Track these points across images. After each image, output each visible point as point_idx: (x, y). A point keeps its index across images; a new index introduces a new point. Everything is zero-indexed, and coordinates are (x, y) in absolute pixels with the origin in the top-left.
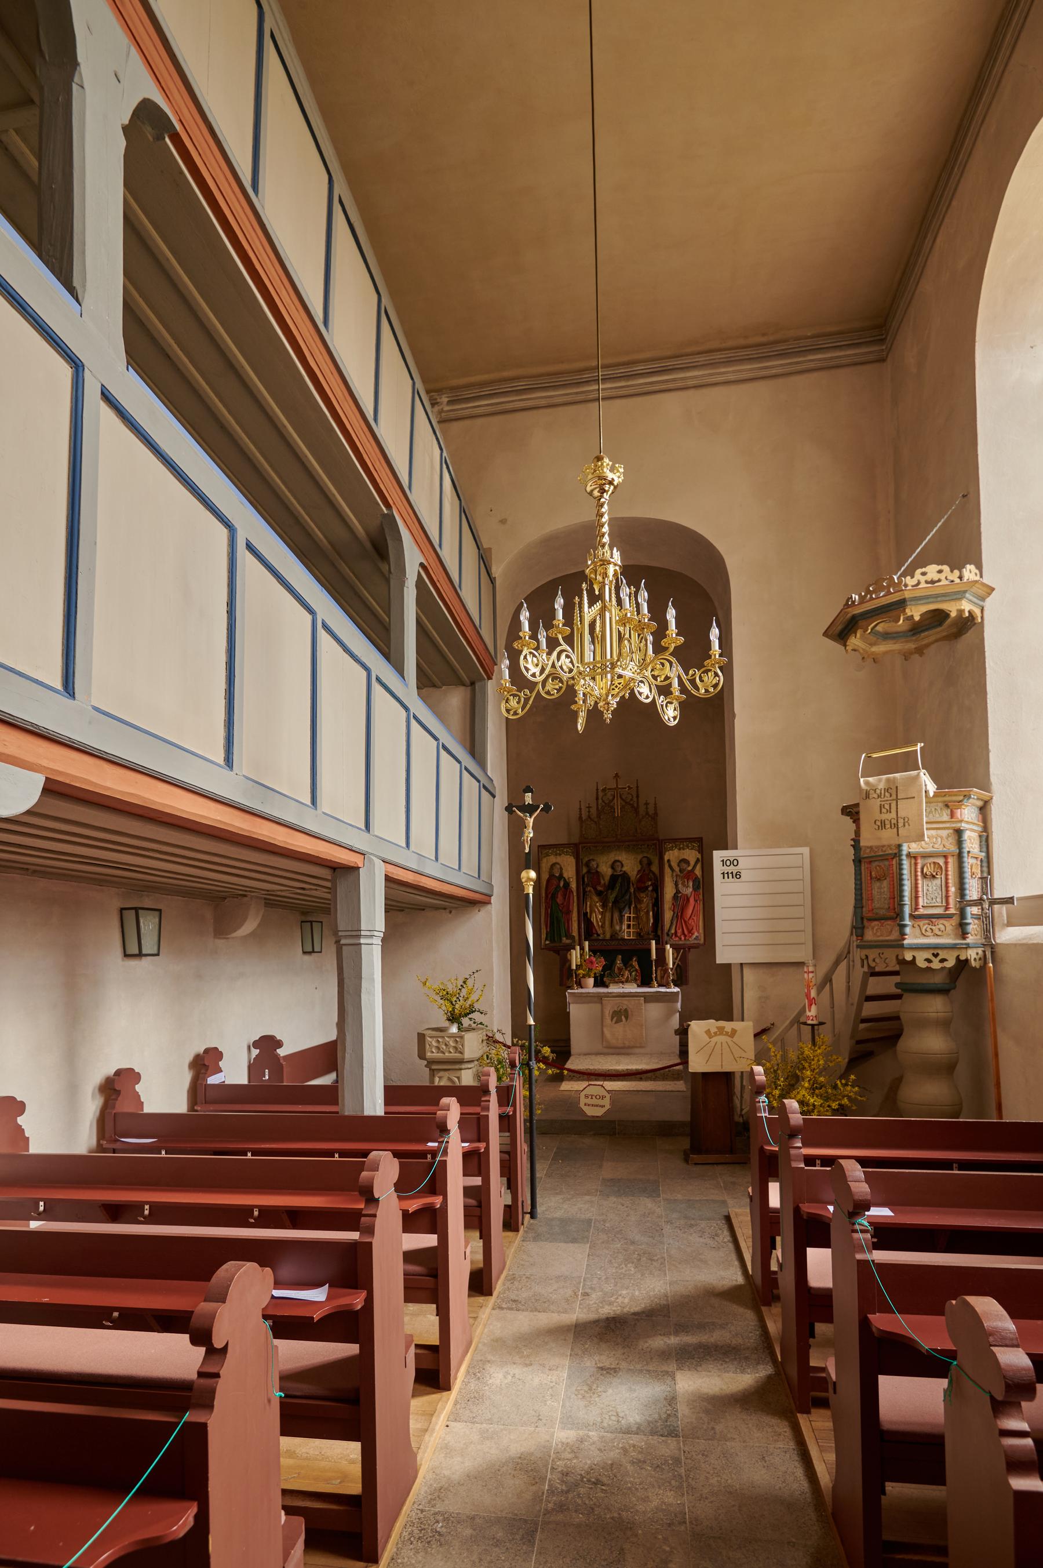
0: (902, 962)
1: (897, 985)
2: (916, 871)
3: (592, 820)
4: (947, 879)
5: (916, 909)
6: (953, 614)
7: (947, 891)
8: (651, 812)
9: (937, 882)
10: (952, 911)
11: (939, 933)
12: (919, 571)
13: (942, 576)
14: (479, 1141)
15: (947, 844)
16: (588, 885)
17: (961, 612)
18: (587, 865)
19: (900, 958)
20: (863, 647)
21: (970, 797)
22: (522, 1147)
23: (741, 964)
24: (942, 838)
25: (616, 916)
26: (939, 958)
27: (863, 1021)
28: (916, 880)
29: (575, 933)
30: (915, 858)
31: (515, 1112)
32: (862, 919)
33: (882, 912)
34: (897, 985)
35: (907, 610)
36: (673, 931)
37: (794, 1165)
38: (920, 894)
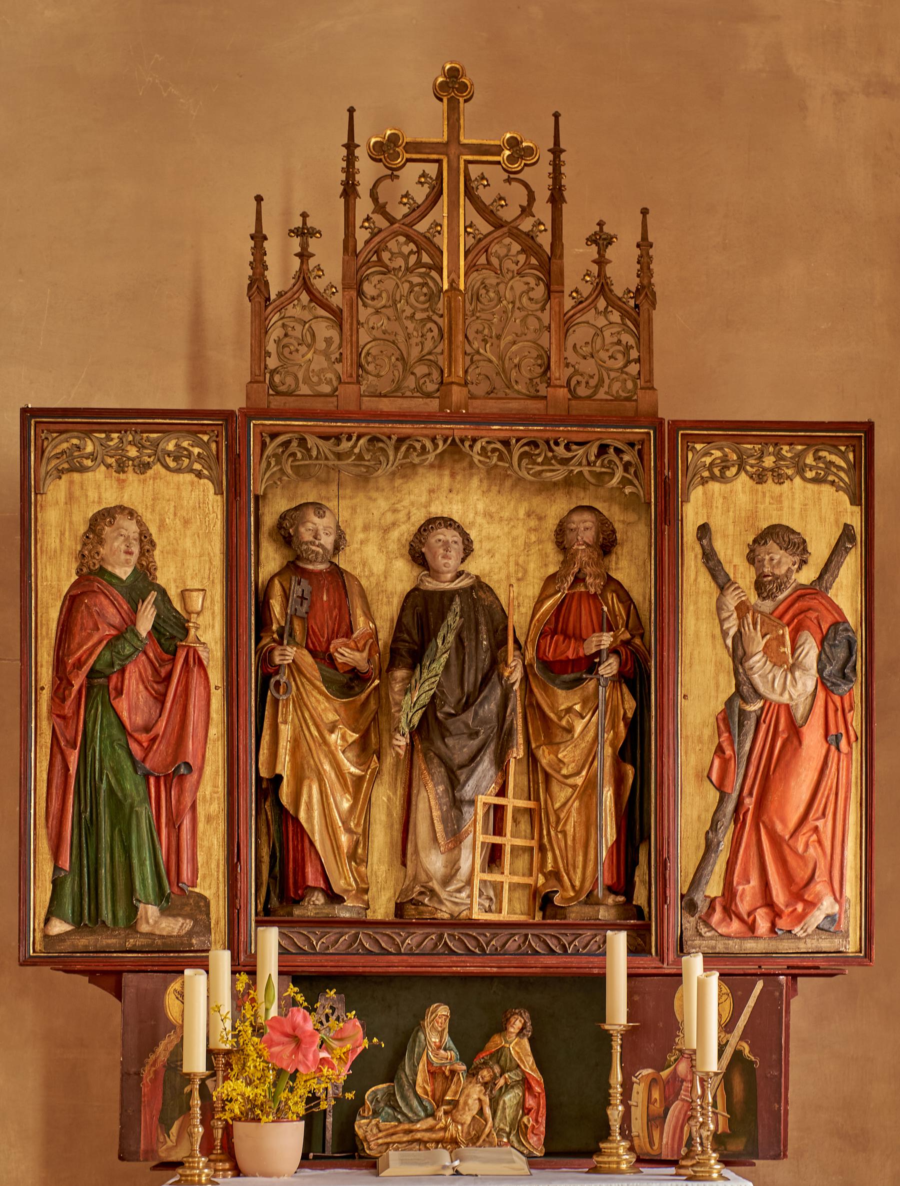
8: (623, 275)
16: (284, 636)
18: (286, 535)
25: (430, 799)
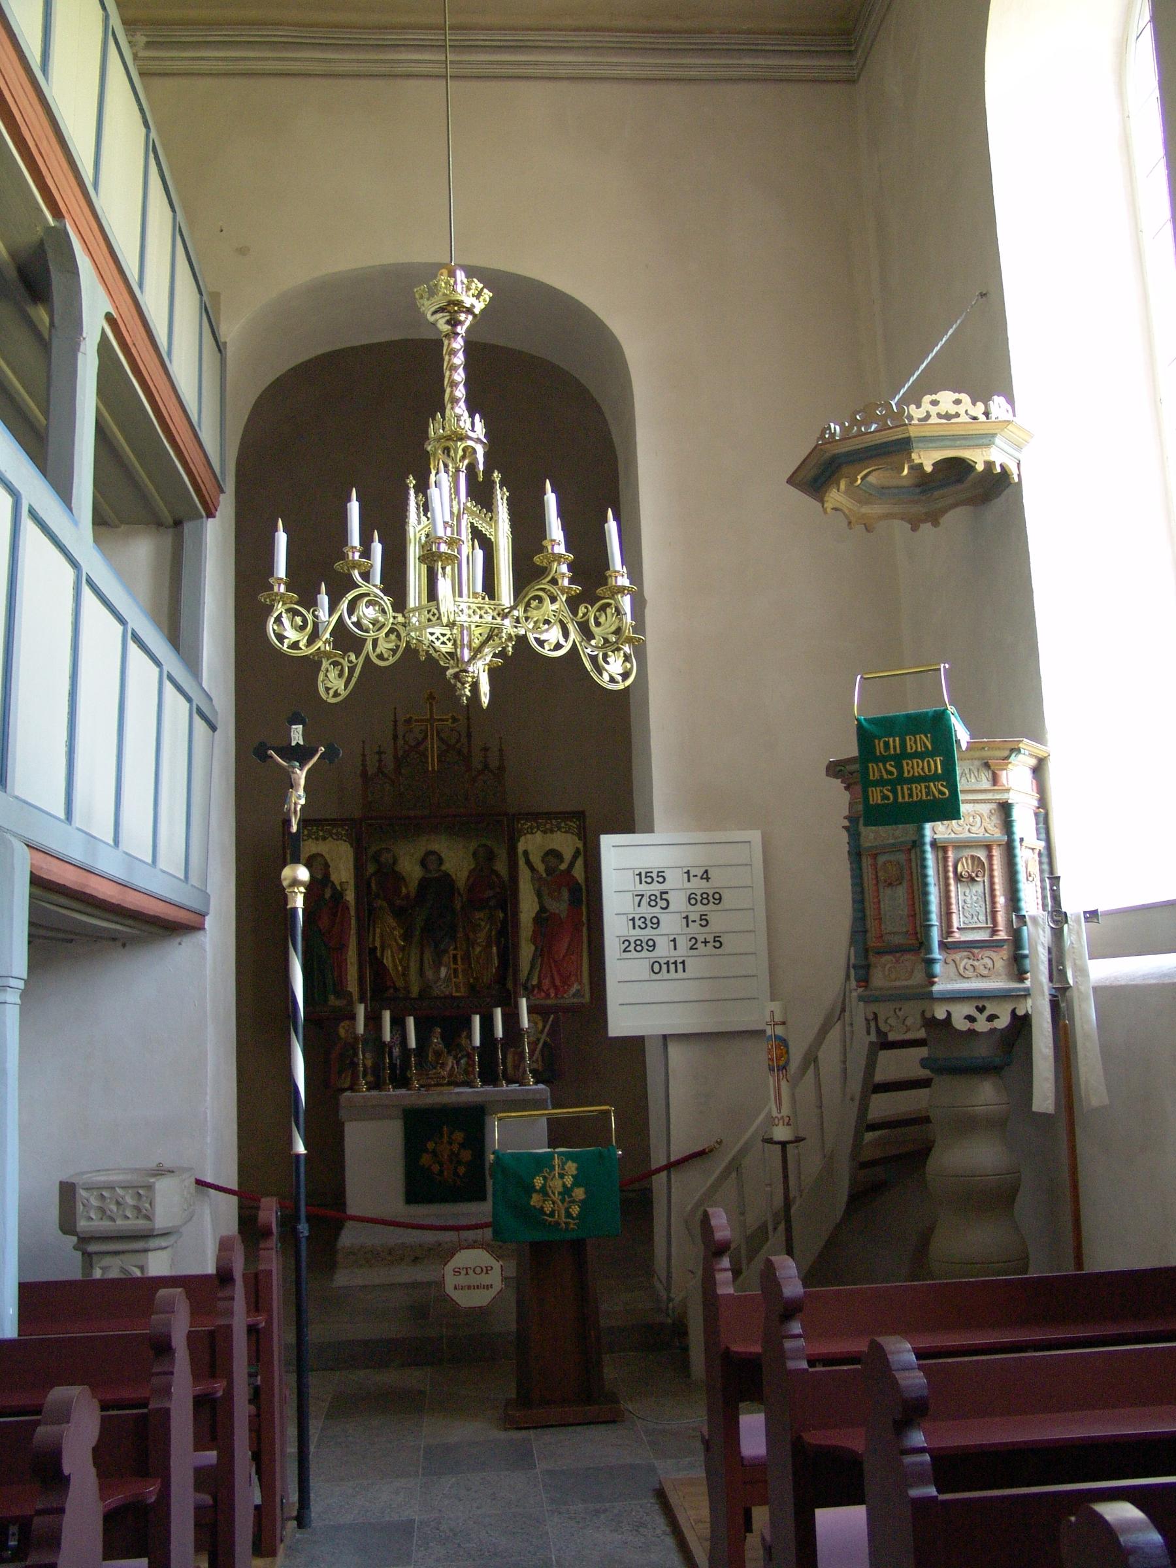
0: (931, 1023)
1: (924, 1063)
2: (946, 871)
3: (385, 775)
4: (992, 884)
5: (950, 933)
6: (980, 467)
7: (993, 903)
8: (494, 763)
9: (978, 889)
10: (1002, 935)
11: (985, 972)
12: (927, 399)
13: (961, 409)
14: (213, 1375)
15: (990, 827)
16: (377, 896)
17: (989, 465)
18: (376, 858)
19: (928, 1015)
20: (849, 505)
21: (1019, 750)
22: (284, 1384)
23: (665, 1037)
24: (981, 816)
25: (428, 956)
26: (987, 1013)
27: (872, 1127)
28: (947, 885)
29: (353, 987)
30: (945, 850)
31: (269, 1321)
32: (866, 950)
33: (897, 940)
34: (924, 1063)
35: (914, 456)
36: (535, 982)
37: (792, 1365)
38: (954, 908)
